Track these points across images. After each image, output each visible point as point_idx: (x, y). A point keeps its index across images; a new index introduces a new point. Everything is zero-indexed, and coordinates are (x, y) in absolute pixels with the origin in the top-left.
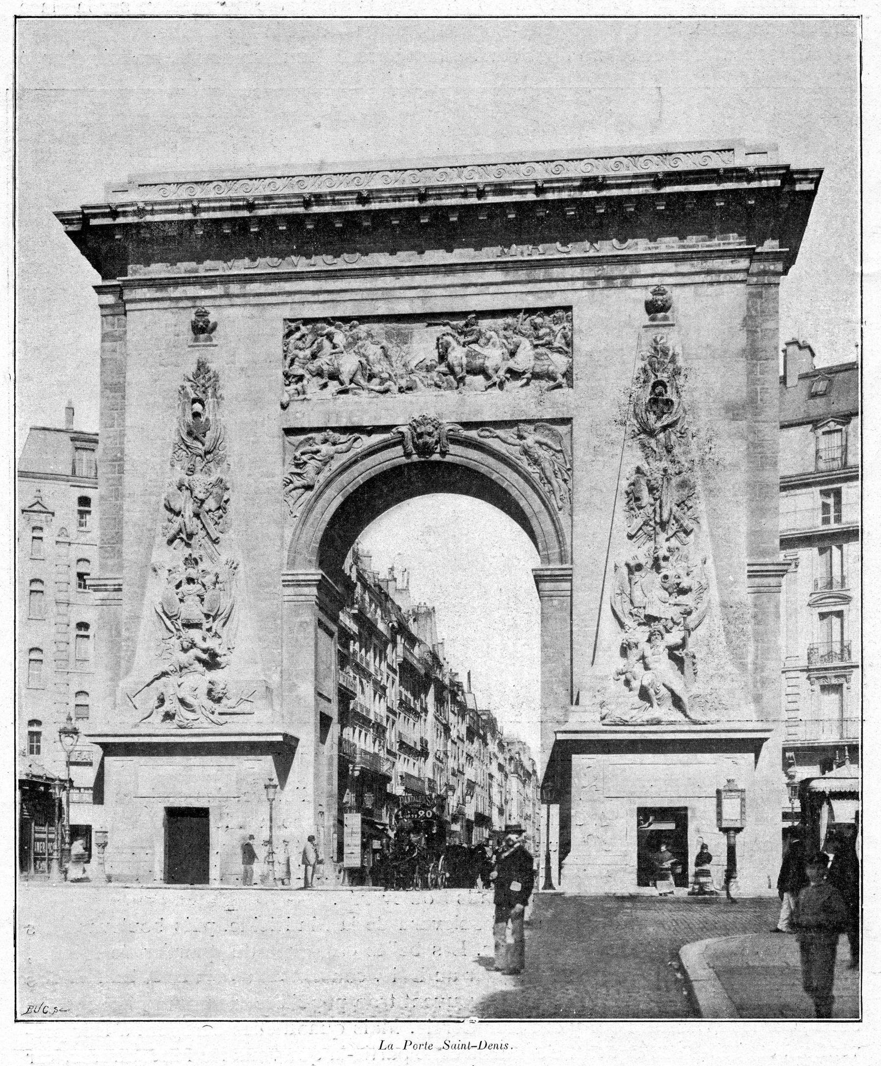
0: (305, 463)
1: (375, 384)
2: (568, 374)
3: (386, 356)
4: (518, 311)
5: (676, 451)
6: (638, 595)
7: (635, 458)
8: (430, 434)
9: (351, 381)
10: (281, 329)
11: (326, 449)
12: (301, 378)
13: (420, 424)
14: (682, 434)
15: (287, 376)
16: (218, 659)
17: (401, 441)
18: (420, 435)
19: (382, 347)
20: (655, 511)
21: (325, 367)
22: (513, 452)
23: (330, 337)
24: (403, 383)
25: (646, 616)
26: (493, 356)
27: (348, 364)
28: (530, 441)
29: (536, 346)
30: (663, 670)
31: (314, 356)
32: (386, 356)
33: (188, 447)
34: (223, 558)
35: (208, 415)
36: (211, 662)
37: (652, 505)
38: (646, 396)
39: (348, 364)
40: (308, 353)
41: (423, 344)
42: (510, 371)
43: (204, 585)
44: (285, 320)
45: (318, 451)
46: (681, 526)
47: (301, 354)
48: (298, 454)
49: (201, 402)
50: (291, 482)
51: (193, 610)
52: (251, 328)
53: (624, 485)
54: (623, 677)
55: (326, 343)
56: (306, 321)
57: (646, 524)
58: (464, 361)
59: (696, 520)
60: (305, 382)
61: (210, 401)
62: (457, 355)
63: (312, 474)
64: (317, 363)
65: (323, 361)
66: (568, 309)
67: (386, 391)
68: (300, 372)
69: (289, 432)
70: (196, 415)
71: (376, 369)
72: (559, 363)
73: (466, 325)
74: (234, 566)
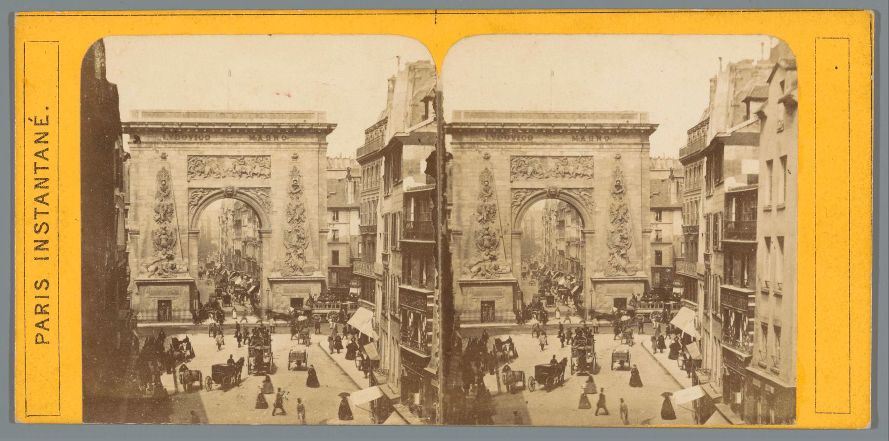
1: (215, 175)
7: (289, 200)
17: (222, 192)
27: (207, 169)
28: (259, 193)
64: (197, 169)
65: (199, 168)
69: (190, 189)
72: (266, 172)
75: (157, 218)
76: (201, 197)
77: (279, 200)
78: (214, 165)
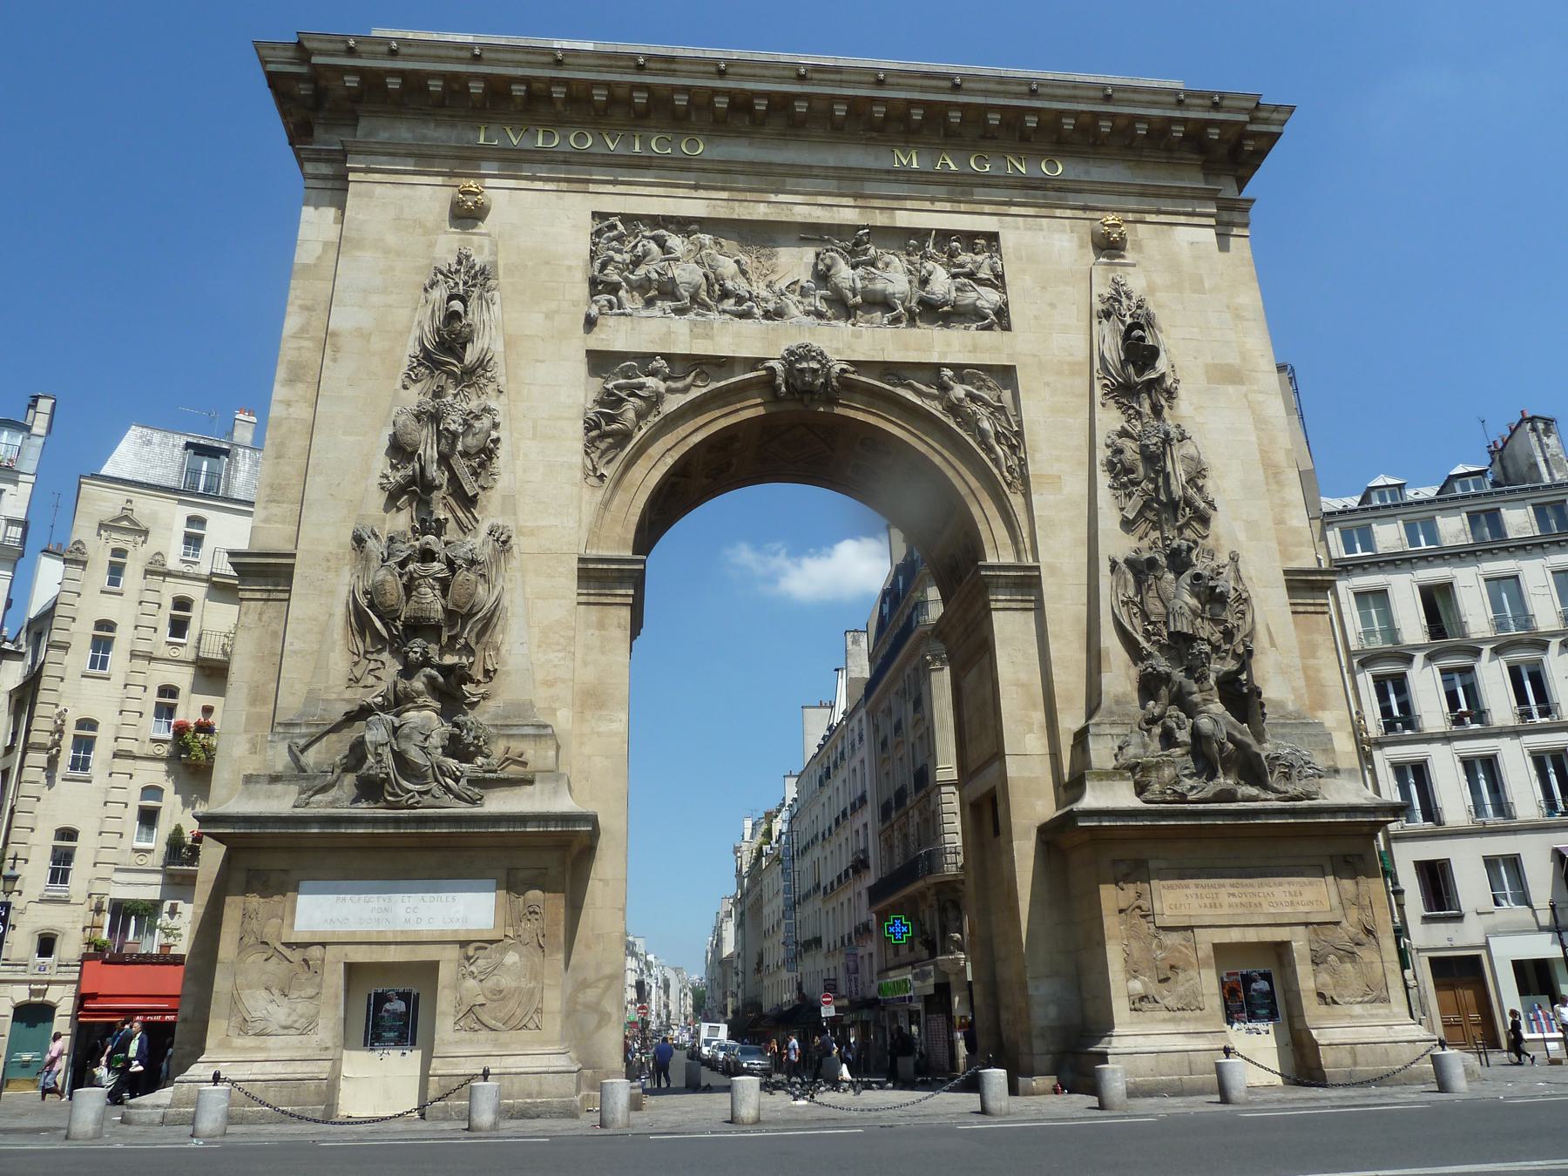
0: (621, 400)
1: (729, 304)
2: (1002, 313)
3: (744, 273)
4: (928, 232)
5: (1166, 413)
6: (1154, 606)
7: (1111, 419)
8: (815, 371)
9: (694, 298)
10: (588, 225)
11: (651, 382)
12: (613, 288)
13: (802, 358)
14: (1171, 395)
15: (593, 282)
16: (467, 688)
18: (802, 371)
19: (737, 262)
20: (1157, 489)
21: (654, 276)
22: (934, 407)
23: (661, 243)
24: (771, 306)
28: (959, 391)
29: (954, 276)
30: (1215, 715)
31: (637, 262)
32: (744, 273)
33: (433, 361)
34: (484, 529)
35: (475, 315)
36: (451, 693)
37: (1151, 480)
38: (1112, 347)
39: (687, 274)
40: (627, 257)
41: (795, 263)
42: (922, 302)
43: (450, 564)
44: (595, 215)
45: (641, 386)
46: (1196, 510)
47: (618, 257)
48: (610, 386)
49: (464, 300)
50: (597, 426)
51: (432, 602)
52: (542, 225)
53: (1102, 454)
54: (1157, 730)
55: (653, 246)
56: (627, 219)
57: (1146, 506)
58: (859, 285)
59: (1211, 504)
60: (622, 293)
61: (473, 303)
62: (845, 274)
63: (631, 415)
64: (641, 271)
66: (992, 238)
67: (747, 315)
68: (616, 278)
70: (453, 316)
71: (729, 285)
72: (988, 298)
73: (856, 244)
74: (503, 538)
75: (397, 477)
76: (655, 400)
77: (1062, 428)
78: (727, 266)
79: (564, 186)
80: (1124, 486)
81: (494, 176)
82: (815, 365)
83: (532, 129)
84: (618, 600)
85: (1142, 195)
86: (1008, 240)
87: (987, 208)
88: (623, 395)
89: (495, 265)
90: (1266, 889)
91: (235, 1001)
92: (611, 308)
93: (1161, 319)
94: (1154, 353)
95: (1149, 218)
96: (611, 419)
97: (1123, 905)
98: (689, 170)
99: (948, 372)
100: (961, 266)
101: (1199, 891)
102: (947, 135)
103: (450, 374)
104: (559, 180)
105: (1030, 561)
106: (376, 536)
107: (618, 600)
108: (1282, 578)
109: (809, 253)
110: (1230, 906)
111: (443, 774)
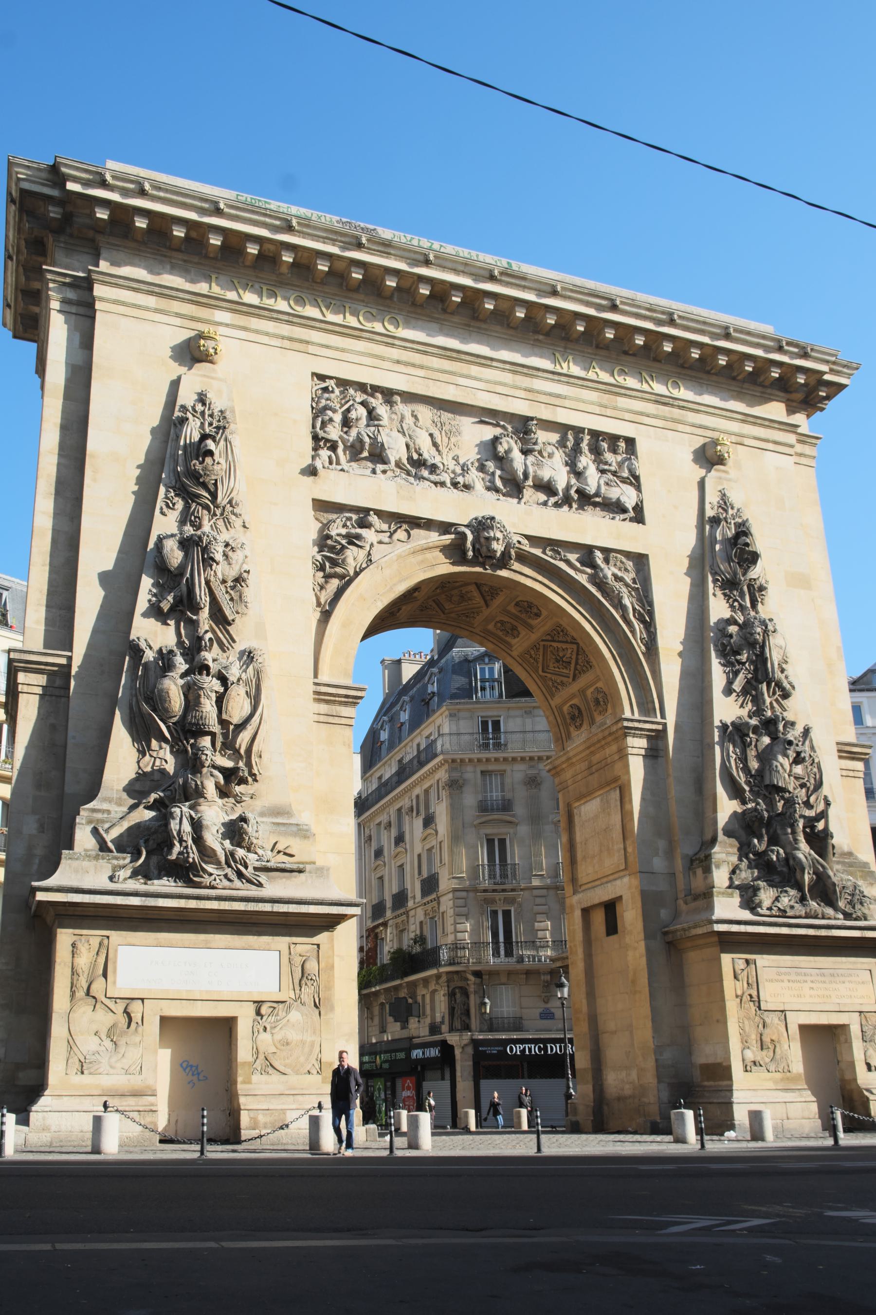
0: (343, 547)
2: (639, 509)
15: (316, 438)
19: (431, 435)
21: (367, 440)
25: (767, 786)
26: (556, 471)
29: (603, 472)
43: (223, 679)
44: (314, 374)
45: (358, 537)
48: (333, 533)
59: (793, 688)
79: (287, 344)
80: (732, 664)
81: (227, 325)
82: (499, 535)
83: (257, 286)
84: (344, 721)
85: (743, 421)
86: (641, 447)
87: (627, 416)
88: (344, 542)
89: (233, 411)
90: (834, 986)
91: (71, 1044)
92: (331, 463)
93: (754, 530)
94: (754, 558)
95: (747, 441)
96: (334, 563)
97: (739, 993)
98: (393, 345)
99: (598, 554)
100: (606, 463)
101: (791, 984)
102: (597, 347)
103: (207, 508)
104: (283, 338)
105: (659, 719)
106: (151, 648)
107: (344, 721)
108: (835, 748)
109: (488, 433)
110: (811, 996)
111: (235, 861)
